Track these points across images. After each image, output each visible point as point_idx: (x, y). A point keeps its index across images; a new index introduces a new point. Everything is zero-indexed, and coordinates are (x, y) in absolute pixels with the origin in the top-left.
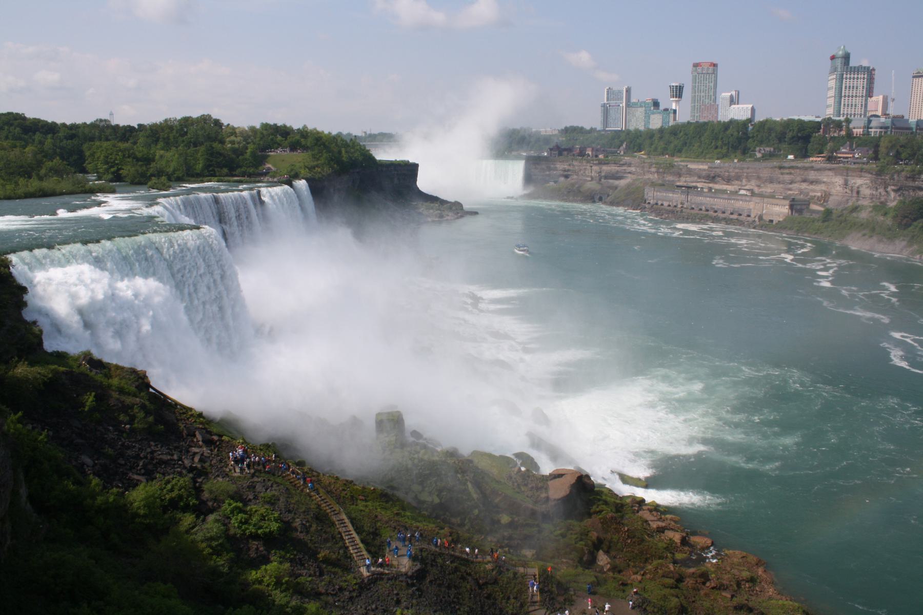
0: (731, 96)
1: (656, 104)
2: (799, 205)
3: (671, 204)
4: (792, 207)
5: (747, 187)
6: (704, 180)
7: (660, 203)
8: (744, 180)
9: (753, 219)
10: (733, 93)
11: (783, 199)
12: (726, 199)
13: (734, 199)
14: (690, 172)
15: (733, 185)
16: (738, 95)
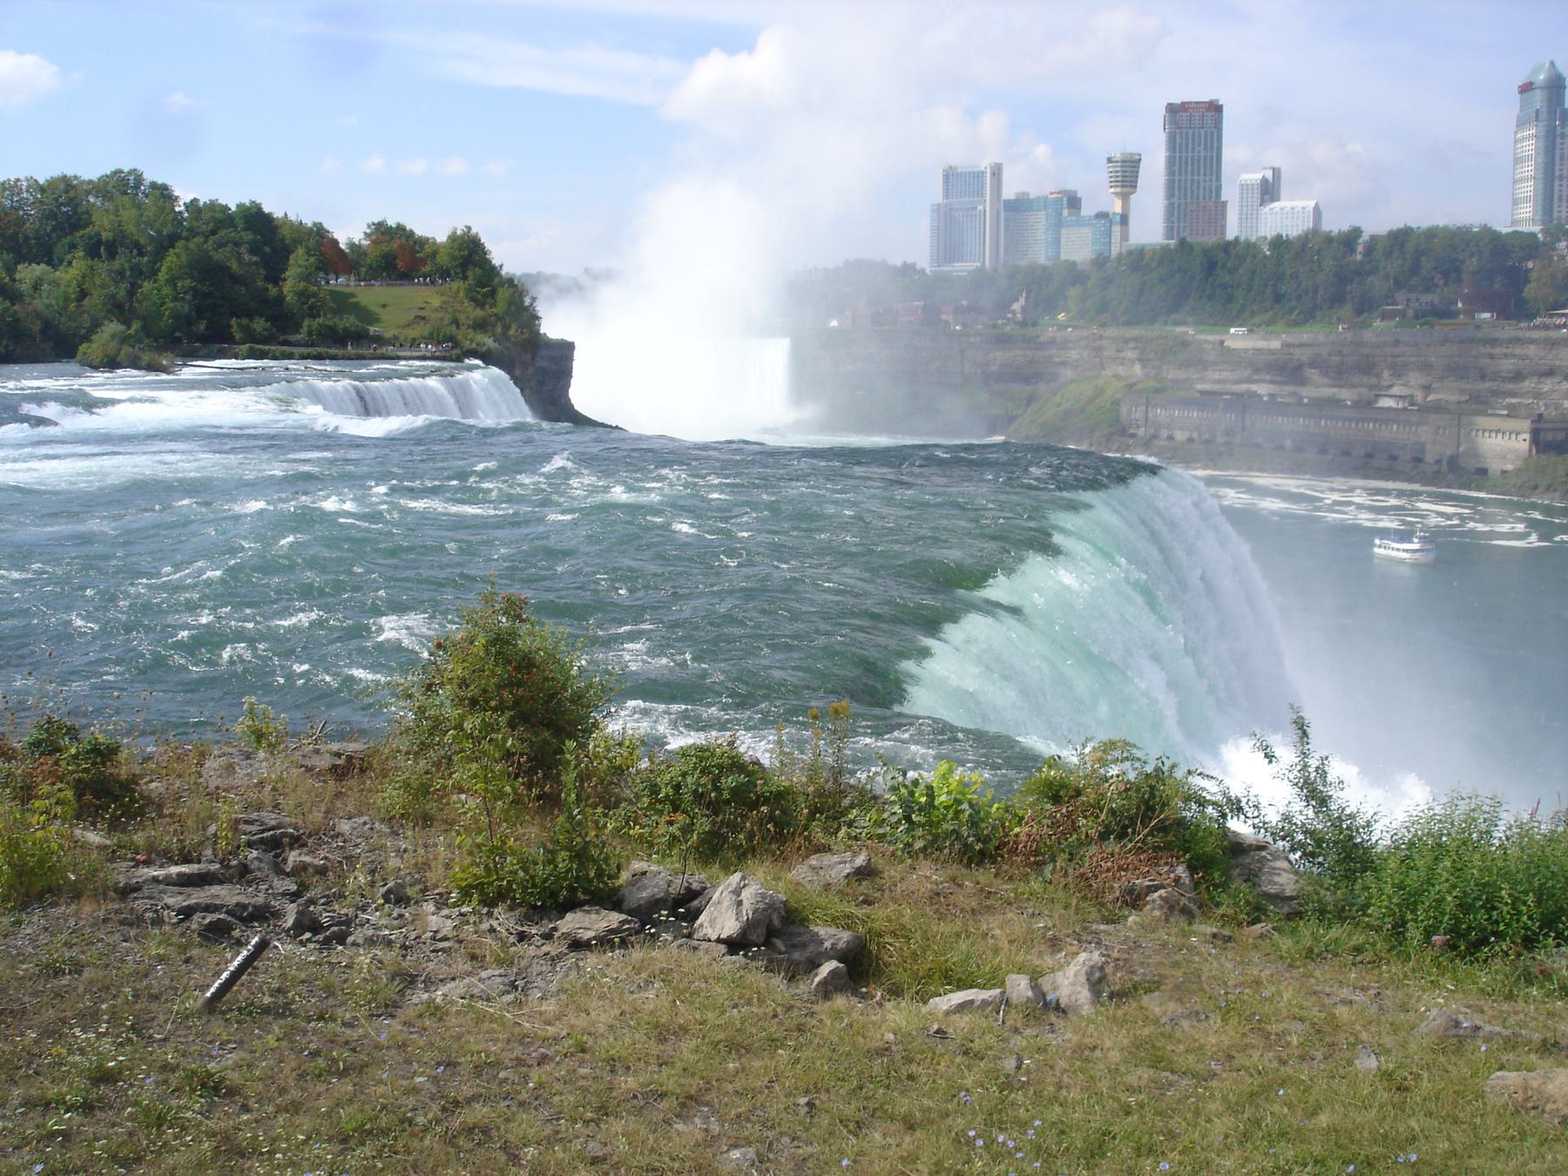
0: (1264, 181)
1: (1074, 202)
2: (1553, 429)
3: (1195, 435)
4: (1536, 435)
5: (1396, 390)
6: (1268, 377)
7: (1164, 433)
8: (1386, 374)
9: (1436, 468)
10: (1269, 175)
11: (1508, 415)
12: (1350, 420)
13: (1375, 421)
14: (1228, 357)
15: (1354, 386)
16: (1279, 178)
